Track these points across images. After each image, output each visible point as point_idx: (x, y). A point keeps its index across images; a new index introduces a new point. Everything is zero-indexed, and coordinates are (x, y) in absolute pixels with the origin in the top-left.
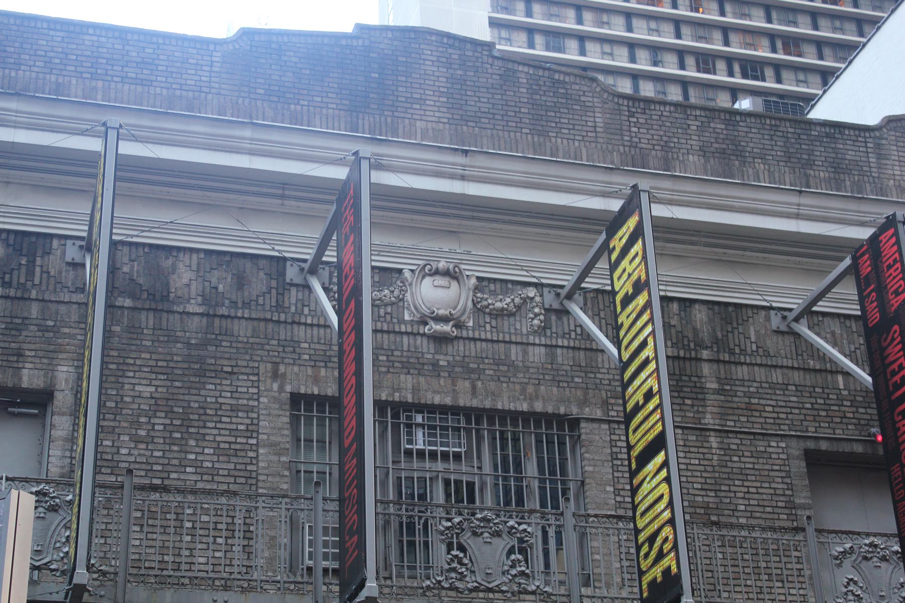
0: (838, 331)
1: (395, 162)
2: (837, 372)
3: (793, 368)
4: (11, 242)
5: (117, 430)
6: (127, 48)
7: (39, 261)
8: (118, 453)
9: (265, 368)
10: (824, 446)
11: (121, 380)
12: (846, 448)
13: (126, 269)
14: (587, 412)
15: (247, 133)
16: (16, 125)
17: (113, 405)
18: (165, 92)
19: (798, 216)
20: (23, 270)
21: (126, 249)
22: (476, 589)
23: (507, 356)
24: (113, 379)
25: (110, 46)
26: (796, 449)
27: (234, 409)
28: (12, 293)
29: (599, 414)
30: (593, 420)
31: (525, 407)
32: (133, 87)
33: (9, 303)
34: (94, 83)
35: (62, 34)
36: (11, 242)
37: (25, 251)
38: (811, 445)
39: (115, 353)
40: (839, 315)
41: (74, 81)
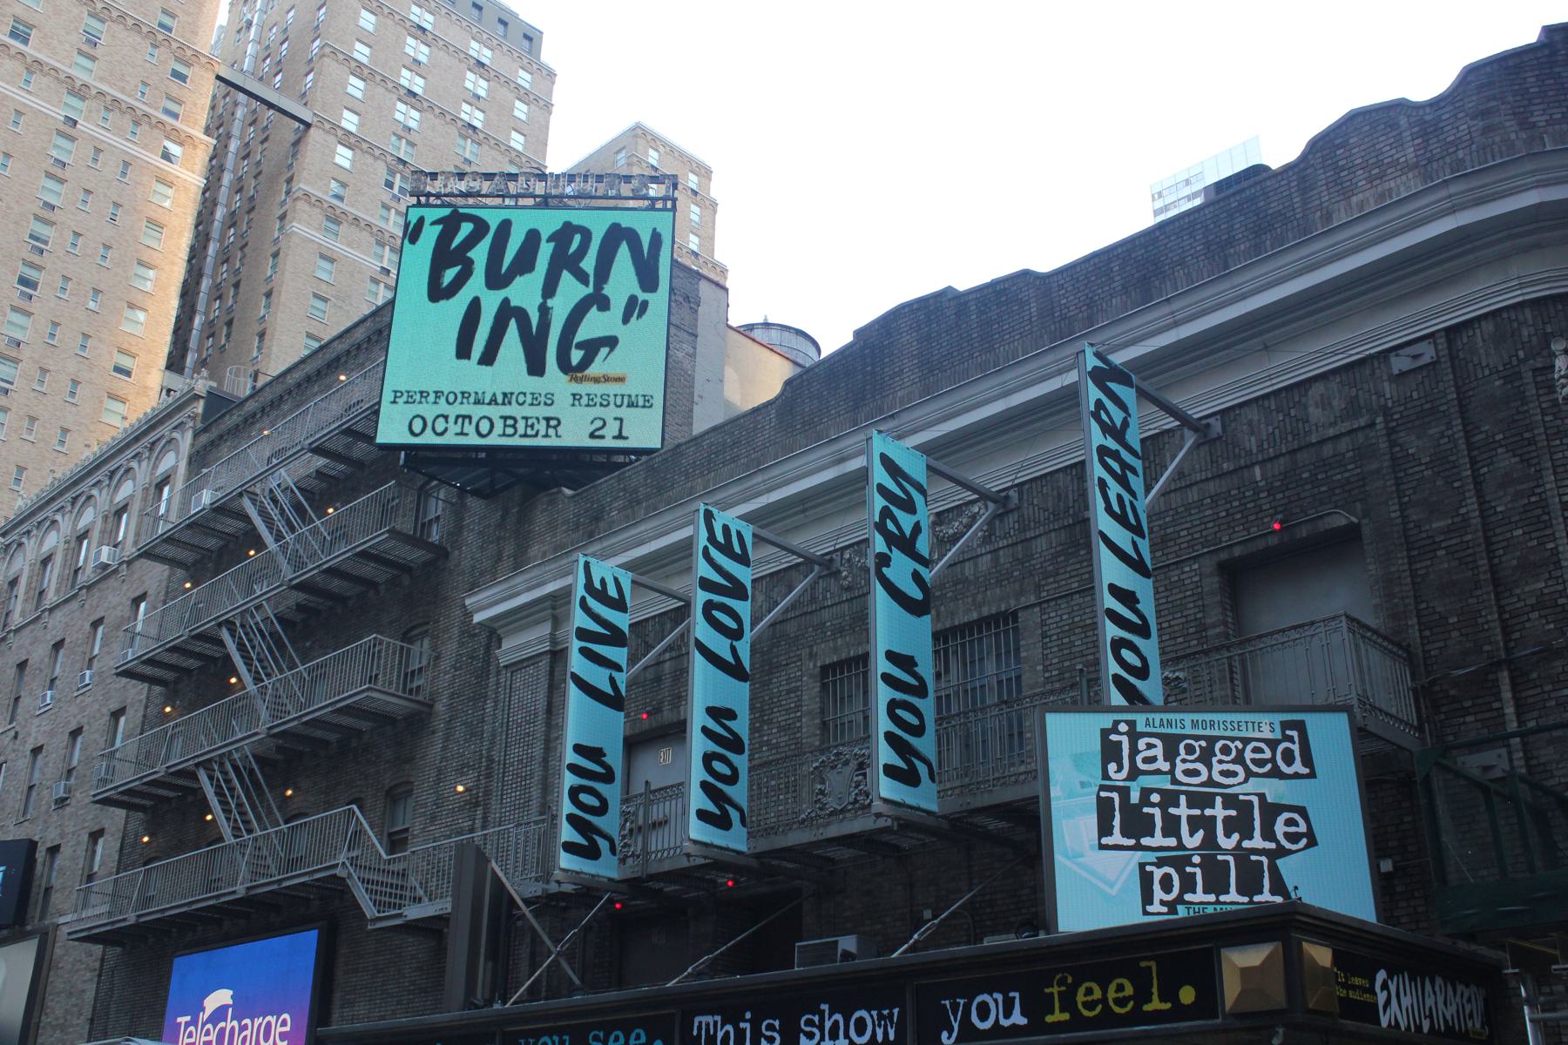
0: (1256, 418)
1: (850, 451)
2: (1253, 464)
3: (1207, 479)
9: (805, 652)
10: (1237, 551)
12: (1261, 544)
14: (1023, 601)
15: (759, 478)
16: (651, 539)
19: (1176, 324)
22: (831, 814)
23: (963, 573)
26: (1209, 564)
27: (789, 692)
29: (1033, 600)
30: (1027, 607)
31: (975, 616)
38: (1224, 556)
40: (1256, 399)
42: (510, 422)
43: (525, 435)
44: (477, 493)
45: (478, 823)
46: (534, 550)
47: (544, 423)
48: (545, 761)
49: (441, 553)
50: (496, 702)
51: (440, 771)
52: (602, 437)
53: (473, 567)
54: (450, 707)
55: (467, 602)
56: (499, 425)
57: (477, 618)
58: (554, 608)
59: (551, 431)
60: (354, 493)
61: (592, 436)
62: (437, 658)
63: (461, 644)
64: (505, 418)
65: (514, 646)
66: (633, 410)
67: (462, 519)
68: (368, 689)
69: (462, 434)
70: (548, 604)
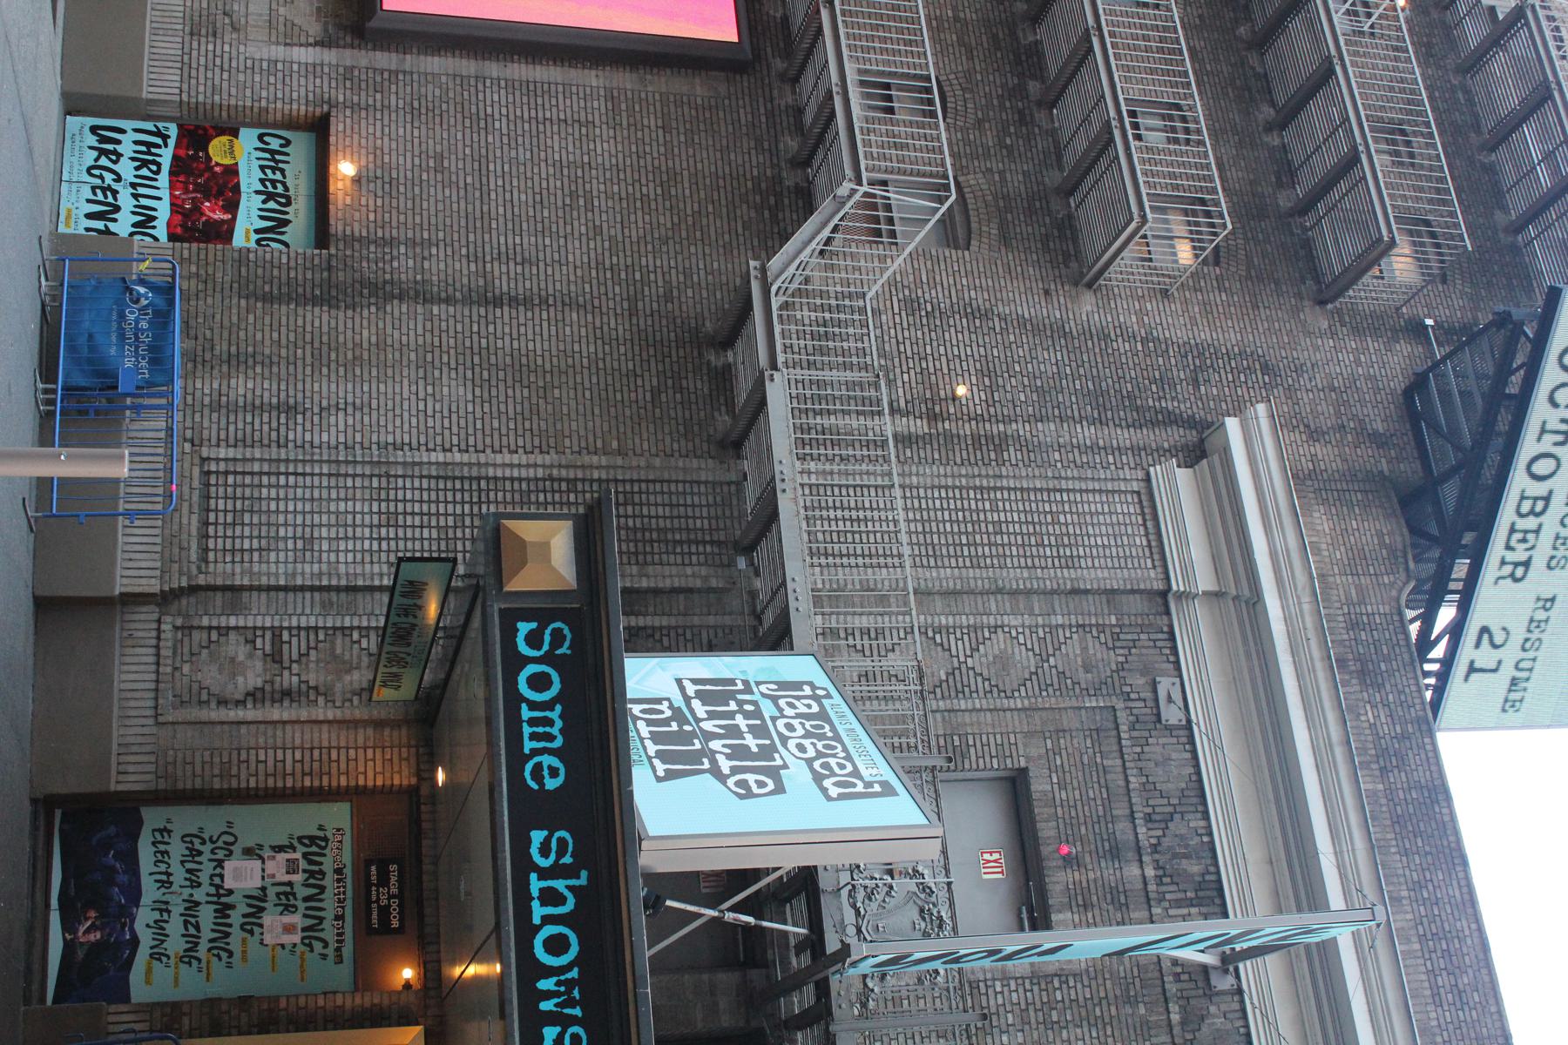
4: (1208, 877)
5: (1027, 1027)
6: (1470, 971)
7: (1194, 910)
8: (1002, 1032)
11: (1085, 1023)
13: (1213, 1009)
17: (1055, 1018)
18: (1434, 1023)
20: (1181, 895)
21: (1236, 1006)
24: (1084, 1014)
25: (1465, 950)
28: (1152, 887)
32: (1426, 984)
33: (1140, 886)
34: (1415, 939)
35: (1457, 894)
36: (1208, 877)
37: (1201, 894)
39: (1113, 1012)
41: (1410, 916)
42: (1540, 506)
43: (1512, 530)
44: (1418, 384)
45: (903, 425)
46: (1321, 520)
47: (1523, 557)
48: (1000, 591)
49: (1327, 292)
50: (1094, 448)
51: (986, 315)
52: (1478, 645)
53: (1299, 370)
54: (1087, 333)
55: (1261, 408)
56: (1539, 489)
57: (1232, 425)
58: (1236, 598)
59: (1508, 569)
60: (1427, 54)
61: (1485, 630)
62: (1165, 293)
63: (1186, 350)
64: (1547, 499)
65: (1179, 487)
66: (1506, 684)
67: (1375, 332)
68: (1144, 218)
69: (1543, 431)
70: (1246, 592)
